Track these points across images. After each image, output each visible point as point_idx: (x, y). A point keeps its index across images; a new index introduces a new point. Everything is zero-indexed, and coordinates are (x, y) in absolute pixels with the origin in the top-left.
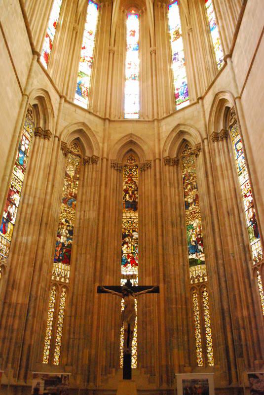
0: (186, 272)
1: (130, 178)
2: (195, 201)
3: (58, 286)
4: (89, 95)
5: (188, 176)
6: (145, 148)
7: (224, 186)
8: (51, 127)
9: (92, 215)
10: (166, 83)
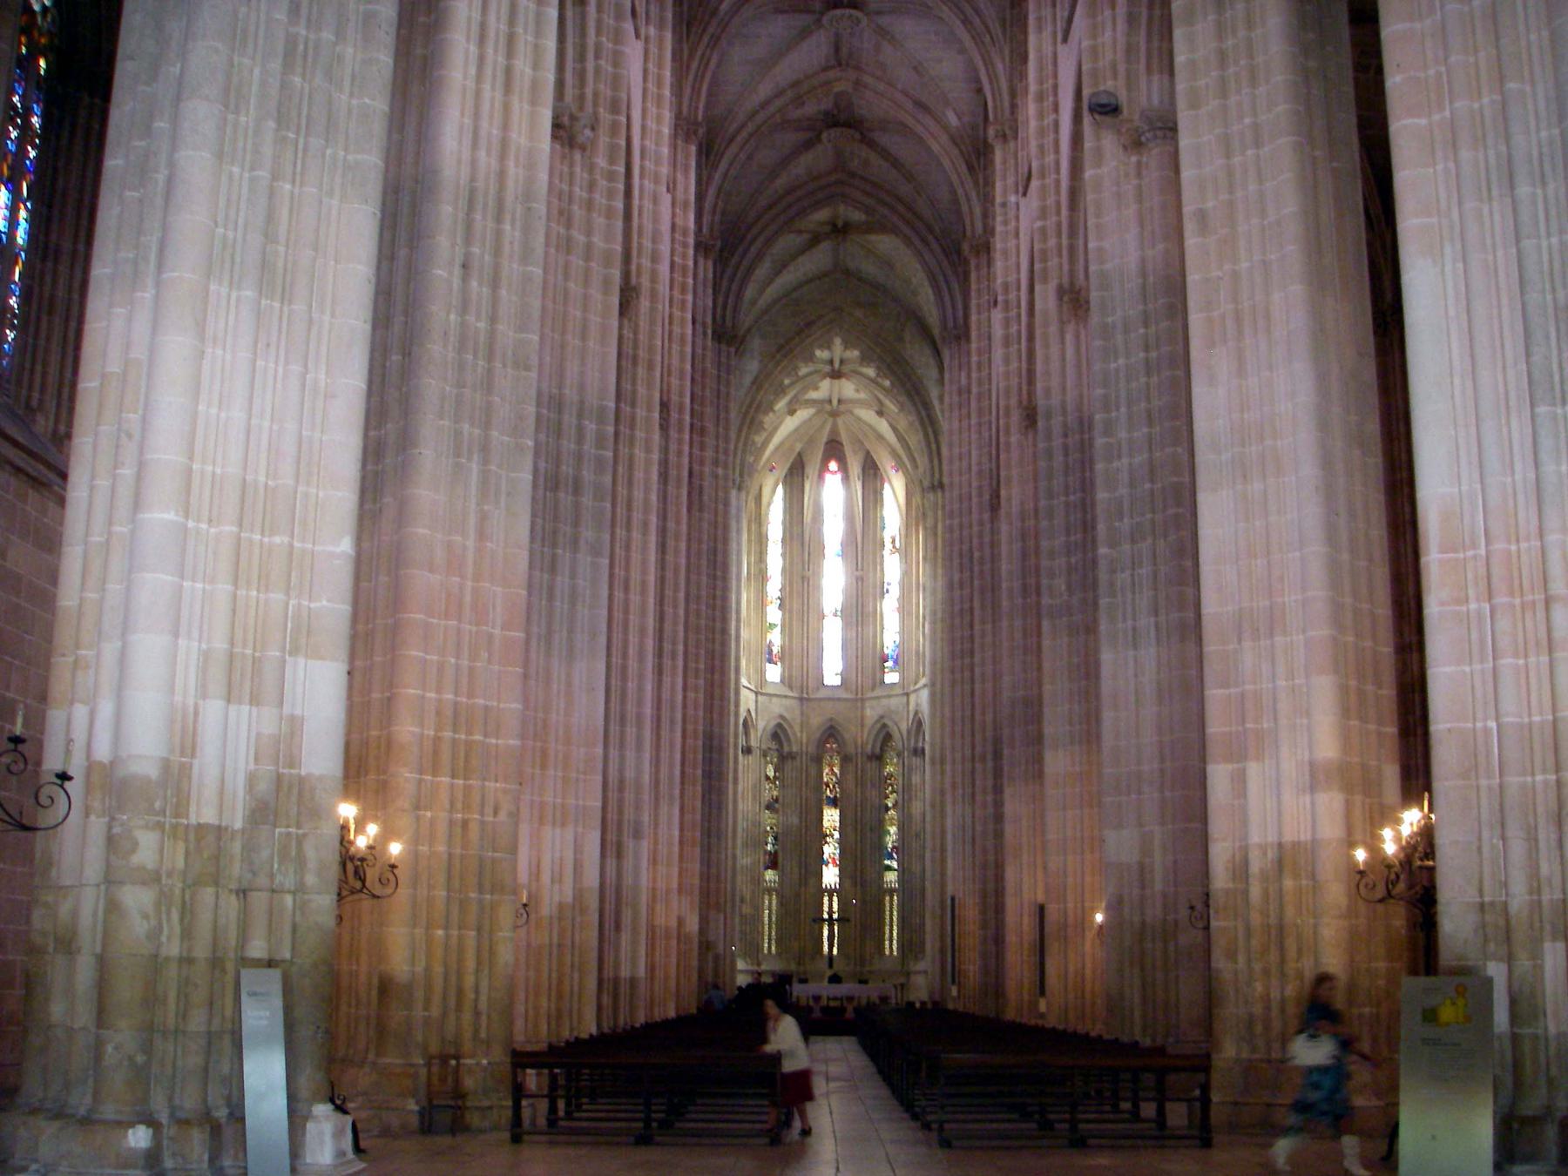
0: (881, 877)
1: (831, 766)
2: (895, 805)
3: (769, 891)
4: (782, 659)
5: (890, 776)
6: (847, 736)
7: (917, 808)
8: (753, 743)
9: (795, 820)
10: (875, 636)
